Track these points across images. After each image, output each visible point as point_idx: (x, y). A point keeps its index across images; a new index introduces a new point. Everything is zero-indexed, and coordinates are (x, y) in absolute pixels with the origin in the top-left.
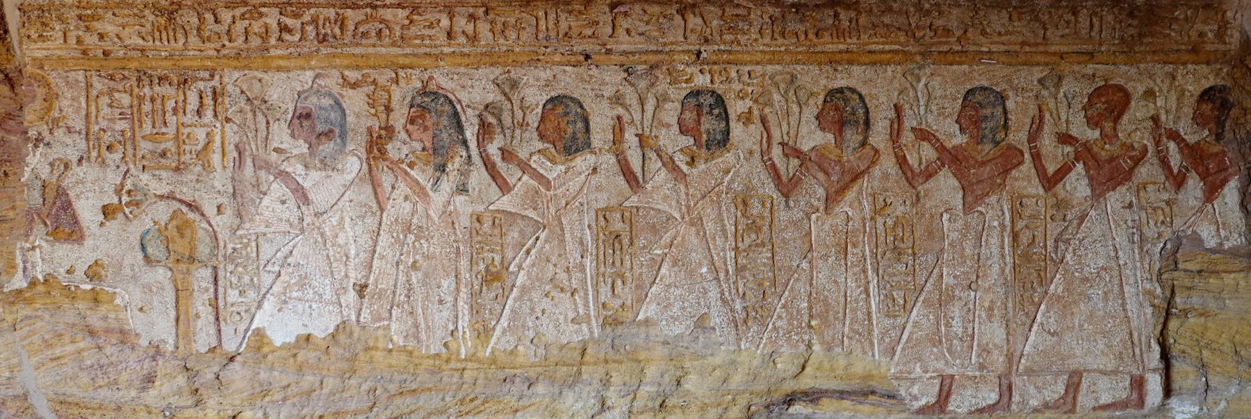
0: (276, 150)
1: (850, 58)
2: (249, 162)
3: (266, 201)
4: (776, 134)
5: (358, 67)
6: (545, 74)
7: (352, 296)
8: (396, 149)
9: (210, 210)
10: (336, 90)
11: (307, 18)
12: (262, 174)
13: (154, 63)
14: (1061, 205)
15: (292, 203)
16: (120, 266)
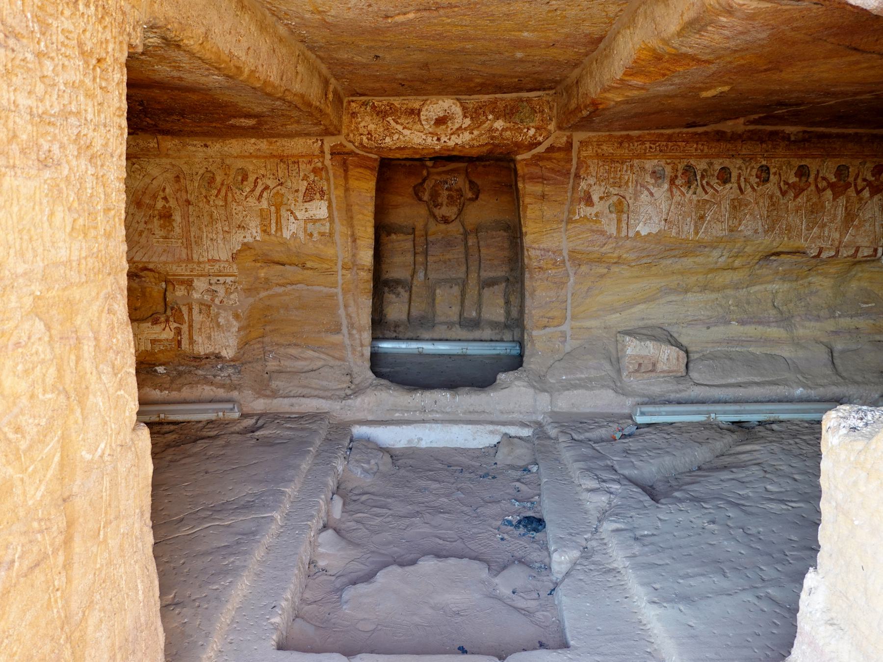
1: (806, 156)
4: (782, 179)
5: (670, 159)
6: (721, 161)
7: (663, 222)
8: (678, 182)
9: (628, 198)
10: (663, 165)
14: (861, 199)
15: (649, 196)
16: (603, 213)
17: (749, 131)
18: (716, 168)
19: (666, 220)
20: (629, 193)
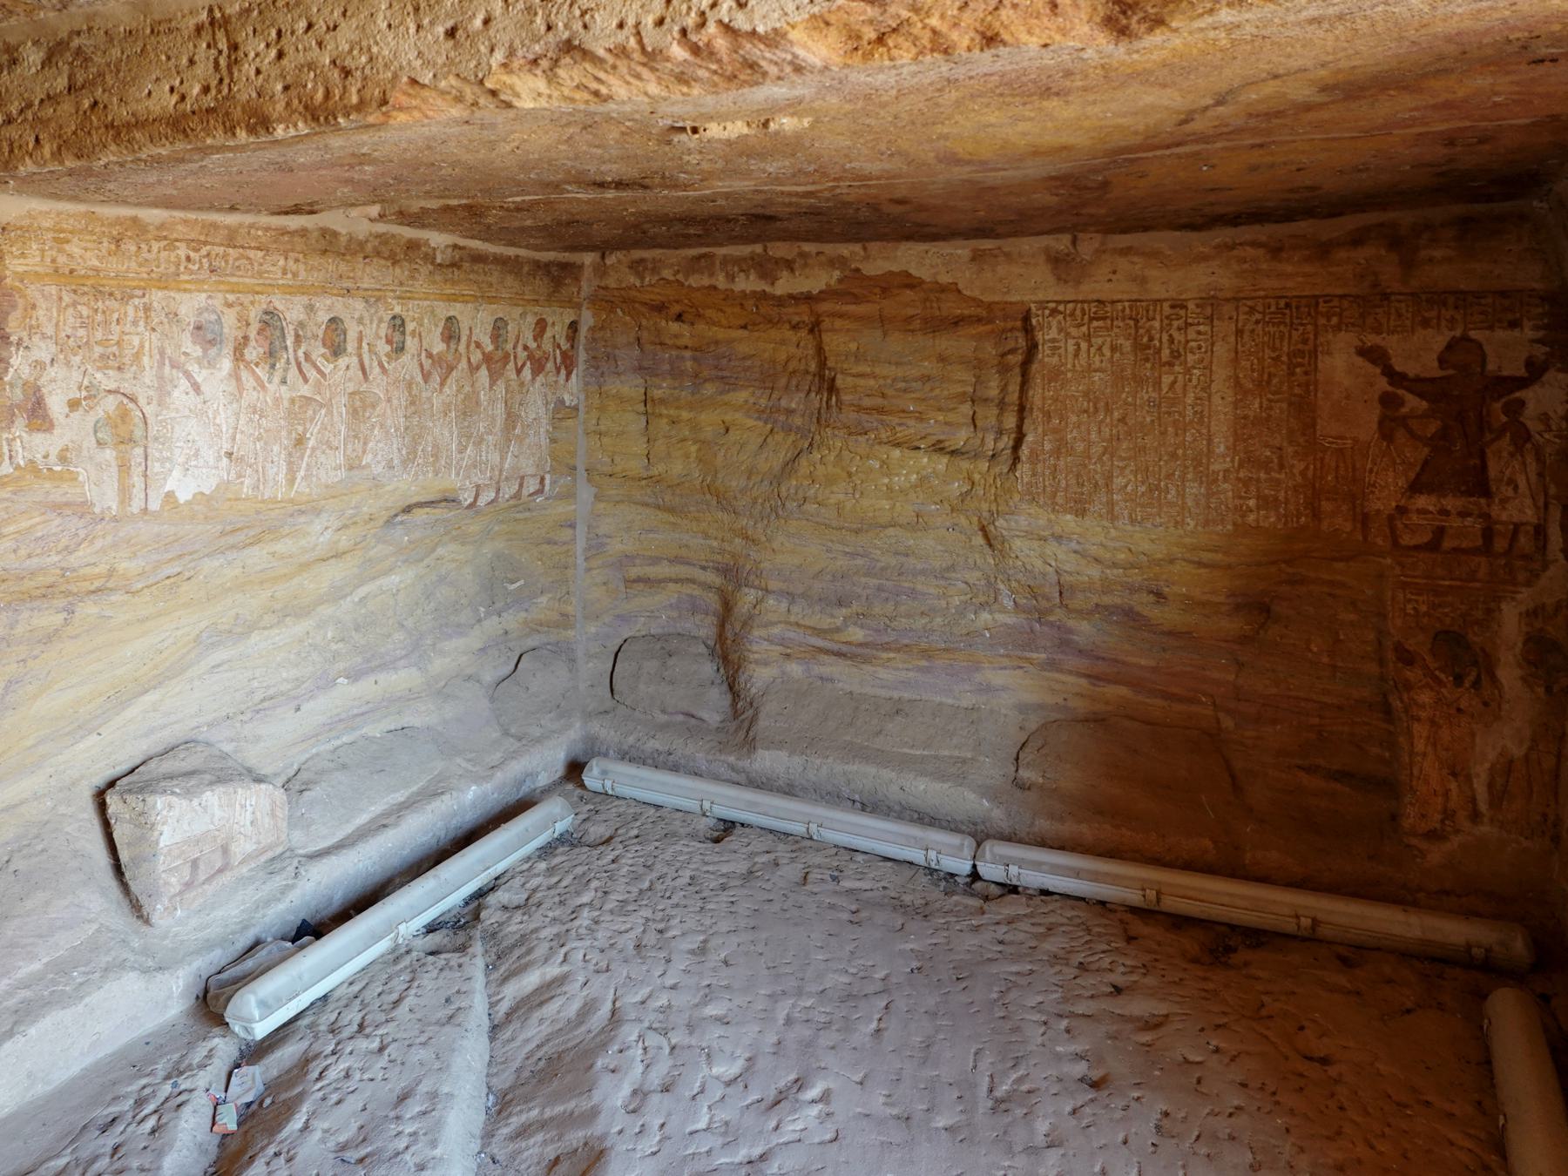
0: (185, 354)
2: (167, 362)
3: (176, 393)
4: (424, 344)
5: (233, 292)
6: (328, 302)
8: (253, 352)
9: (142, 401)
11: (204, 251)
12: (174, 371)
13: (104, 282)
14: (522, 384)
15: (192, 393)
17: (378, 236)
18: (320, 320)
19: (229, 455)
20: (143, 385)
